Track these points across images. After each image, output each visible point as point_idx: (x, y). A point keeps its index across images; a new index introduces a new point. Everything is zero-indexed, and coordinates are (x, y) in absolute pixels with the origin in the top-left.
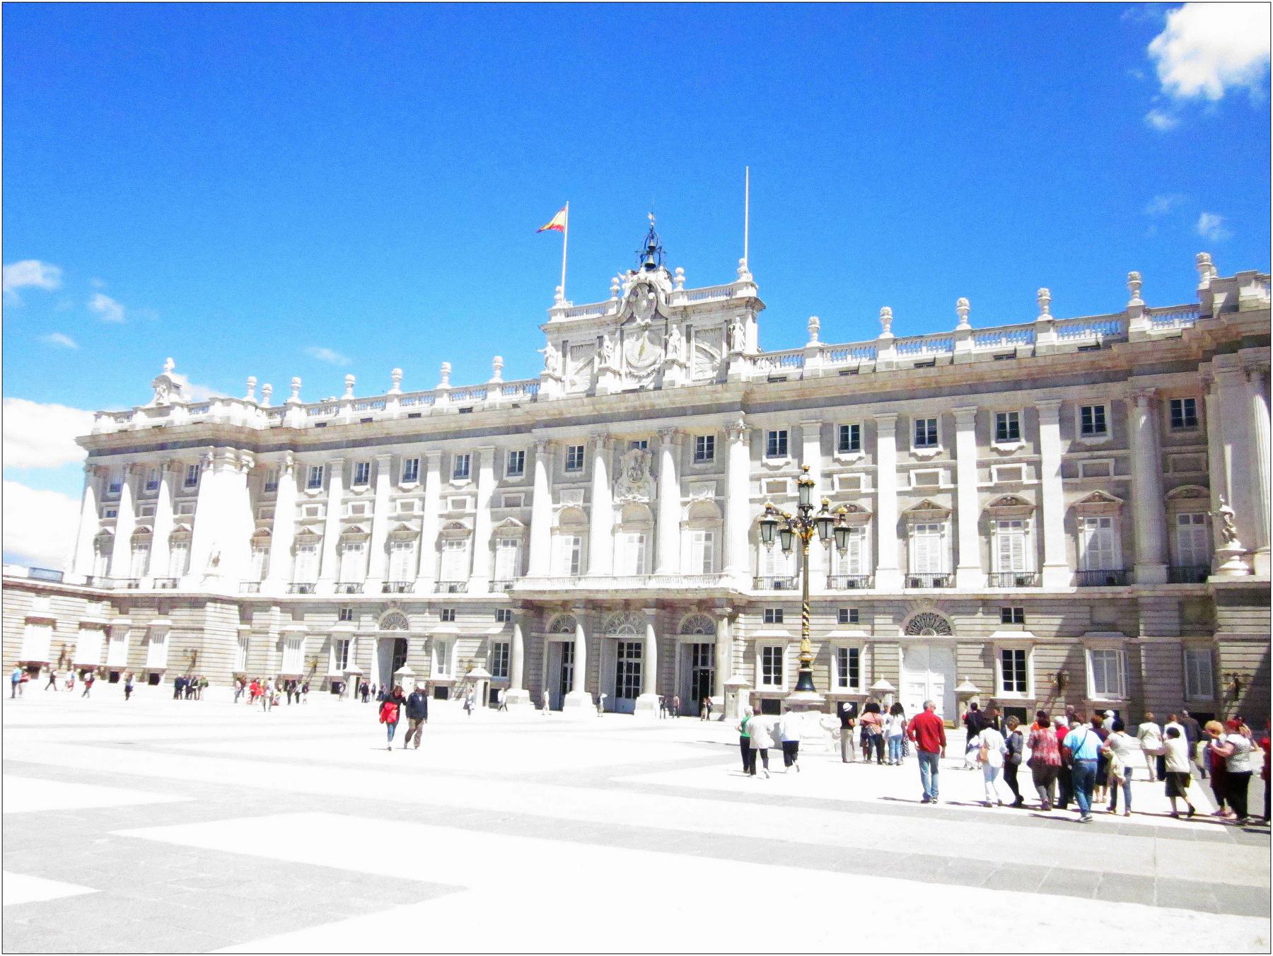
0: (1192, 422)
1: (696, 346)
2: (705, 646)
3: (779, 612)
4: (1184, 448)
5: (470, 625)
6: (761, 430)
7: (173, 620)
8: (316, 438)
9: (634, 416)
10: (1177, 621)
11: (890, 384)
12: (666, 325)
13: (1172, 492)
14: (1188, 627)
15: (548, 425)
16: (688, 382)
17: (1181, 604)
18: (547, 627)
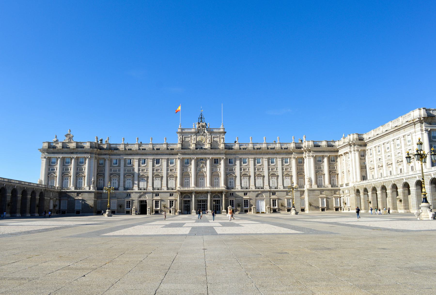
1: (213, 140)
2: (217, 200)
3: (232, 193)
4: (300, 166)
5: (163, 197)
6: (228, 158)
7: (82, 198)
8: (116, 153)
9: (202, 154)
10: (300, 194)
11: (253, 152)
12: (206, 135)
13: (299, 174)
14: (301, 196)
16: (212, 147)
17: (300, 192)
18: (183, 197)
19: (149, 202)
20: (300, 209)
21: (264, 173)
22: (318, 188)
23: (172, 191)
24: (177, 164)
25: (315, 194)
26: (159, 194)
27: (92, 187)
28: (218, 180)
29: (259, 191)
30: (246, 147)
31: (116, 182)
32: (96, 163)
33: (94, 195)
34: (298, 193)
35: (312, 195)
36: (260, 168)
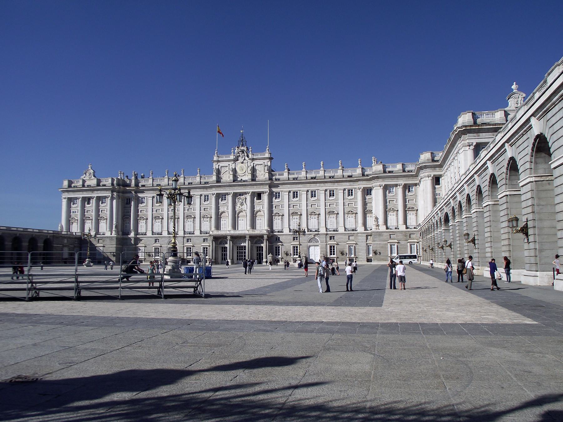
0: (371, 194)
13: (366, 210)
15: (215, 189)
18: (218, 243)
19: (180, 250)
20: (366, 259)
21: (320, 211)
22: (387, 230)
23: (205, 235)
24: (212, 202)
25: (382, 238)
26: (192, 239)
27: (114, 233)
28: (261, 221)
29: (310, 234)
30: (296, 176)
31: (143, 226)
32: (120, 203)
33: (116, 240)
34: (363, 237)
35: (378, 240)
36: (315, 204)
